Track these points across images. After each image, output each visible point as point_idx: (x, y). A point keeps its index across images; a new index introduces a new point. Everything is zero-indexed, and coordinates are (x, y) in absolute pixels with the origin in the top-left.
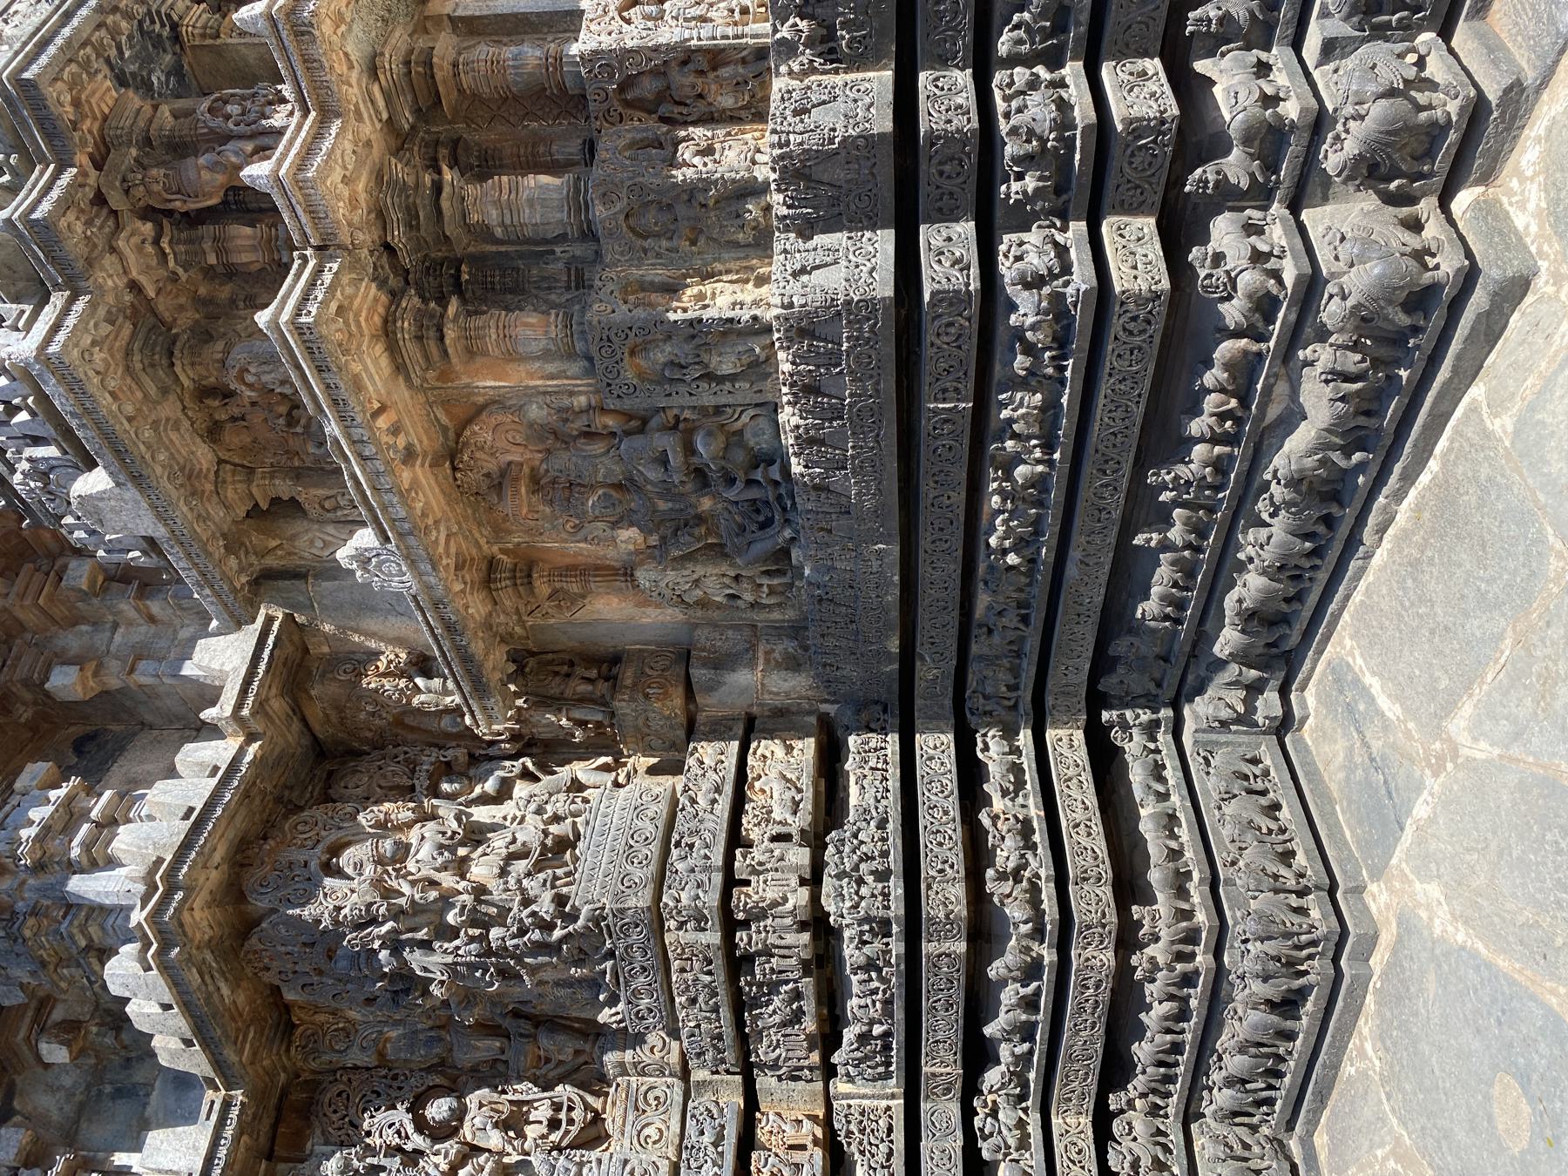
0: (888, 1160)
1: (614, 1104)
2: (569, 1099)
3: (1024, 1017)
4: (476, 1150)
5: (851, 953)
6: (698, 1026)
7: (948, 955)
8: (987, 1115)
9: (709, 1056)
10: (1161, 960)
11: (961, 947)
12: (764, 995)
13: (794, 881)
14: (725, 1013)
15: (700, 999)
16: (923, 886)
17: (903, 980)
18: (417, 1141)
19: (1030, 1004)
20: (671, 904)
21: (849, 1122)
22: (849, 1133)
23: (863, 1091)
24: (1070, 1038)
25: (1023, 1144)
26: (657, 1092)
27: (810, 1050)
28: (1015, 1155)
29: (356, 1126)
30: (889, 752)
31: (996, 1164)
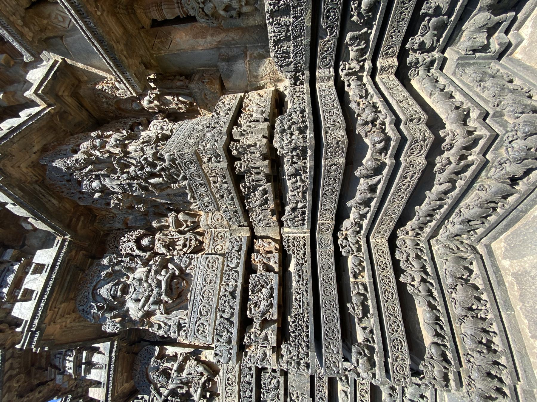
0: (304, 256)
1: (206, 238)
2: (190, 237)
3: (369, 196)
4: (156, 254)
5: (288, 169)
6: (227, 207)
7: (336, 165)
8: (344, 239)
9: (234, 219)
10: (452, 159)
11: (343, 161)
12: (252, 192)
13: (260, 137)
14: (236, 200)
15: (225, 195)
16: (323, 133)
17: (312, 181)
18: (137, 252)
19: (372, 189)
20: (202, 148)
21: (289, 242)
22: (289, 246)
23: (294, 231)
24: (388, 205)
25: (359, 250)
26: (221, 234)
27: (272, 215)
28: (356, 254)
29: (117, 248)
30: (305, 91)
31: (347, 257)
